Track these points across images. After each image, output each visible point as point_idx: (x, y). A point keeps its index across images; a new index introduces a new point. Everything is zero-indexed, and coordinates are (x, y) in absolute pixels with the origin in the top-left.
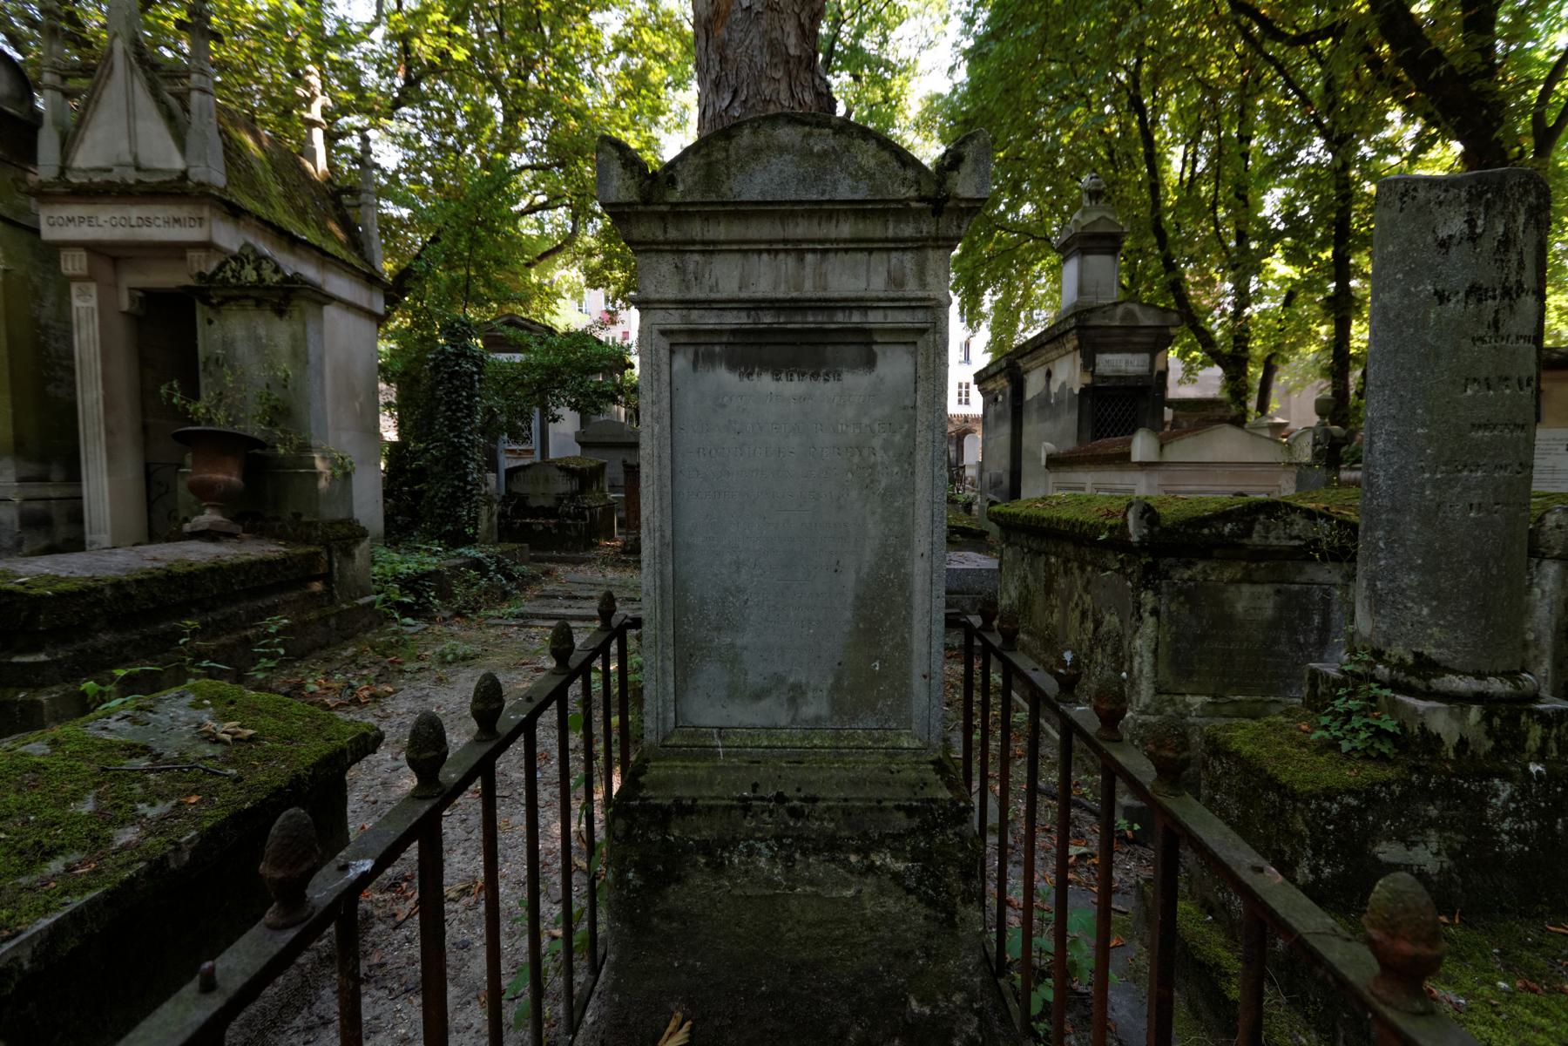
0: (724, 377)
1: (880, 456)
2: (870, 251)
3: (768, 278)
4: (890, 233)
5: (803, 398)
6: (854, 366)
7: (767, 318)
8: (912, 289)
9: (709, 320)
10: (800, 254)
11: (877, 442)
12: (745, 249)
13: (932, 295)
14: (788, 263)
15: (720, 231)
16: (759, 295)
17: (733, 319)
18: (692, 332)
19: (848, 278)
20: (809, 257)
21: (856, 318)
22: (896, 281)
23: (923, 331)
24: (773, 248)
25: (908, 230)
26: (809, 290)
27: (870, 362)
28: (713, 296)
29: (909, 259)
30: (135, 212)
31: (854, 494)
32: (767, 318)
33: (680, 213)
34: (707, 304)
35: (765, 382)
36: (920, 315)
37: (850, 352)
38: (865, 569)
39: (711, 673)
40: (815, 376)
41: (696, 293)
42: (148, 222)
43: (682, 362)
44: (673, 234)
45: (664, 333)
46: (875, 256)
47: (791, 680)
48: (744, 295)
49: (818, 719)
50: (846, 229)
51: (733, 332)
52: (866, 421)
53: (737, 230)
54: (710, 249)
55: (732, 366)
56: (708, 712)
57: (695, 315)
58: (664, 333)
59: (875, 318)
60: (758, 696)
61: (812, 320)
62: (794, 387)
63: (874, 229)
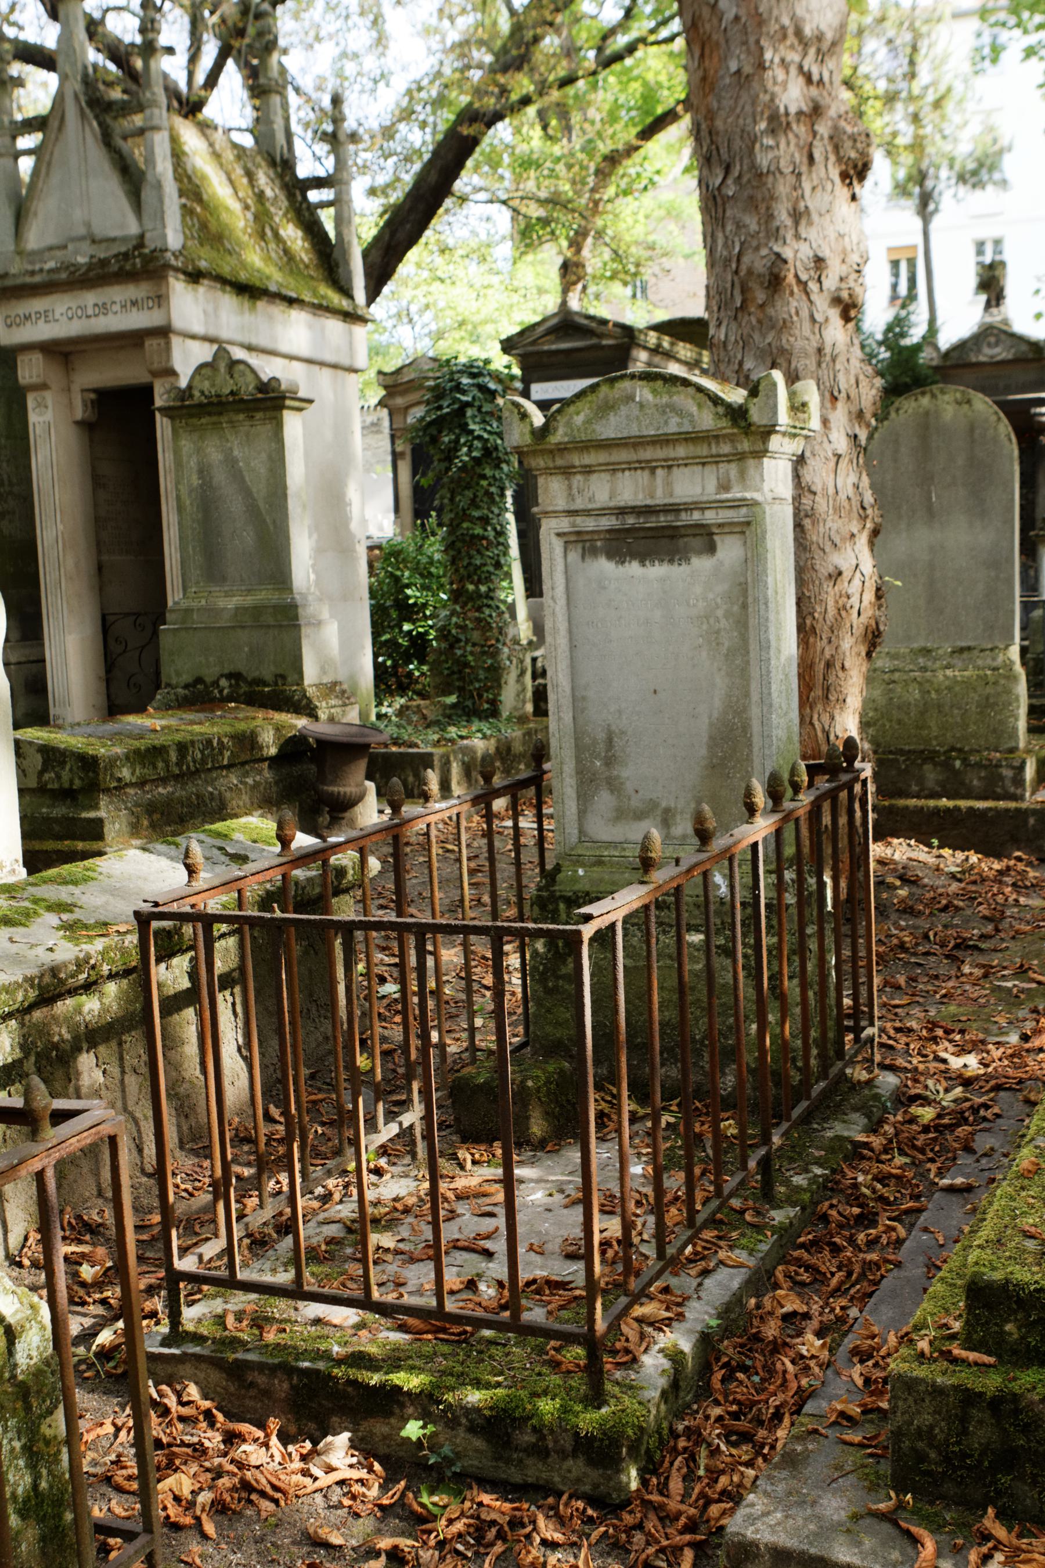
0: (604, 566)
1: (724, 623)
2: (704, 464)
3: (630, 489)
4: (714, 451)
5: (663, 580)
6: (699, 553)
7: (631, 520)
8: (736, 493)
9: (589, 524)
10: (653, 470)
11: (720, 613)
12: (613, 469)
13: (748, 495)
14: (643, 477)
15: (590, 458)
16: (622, 504)
17: (607, 522)
18: (578, 533)
19: (690, 485)
20: (660, 472)
21: (696, 515)
22: (724, 486)
23: (748, 523)
24: (633, 467)
25: (726, 448)
26: (660, 498)
27: (711, 549)
28: (590, 506)
29: (733, 469)
30: (90, 298)
31: (704, 654)
32: (631, 520)
33: (562, 449)
34: (587, 513)
35: (634, 568)
36: (744, 511)
37: (697, 542)
38: (715, 714)
39: (604, 800)
40: (671, 561)
41: (579, 504)
42: (103, 309)
43: (574, 556)
44: (559, 462)
45: (558, 535)
46: (708, 468)
47: (664, 804)
48: (612, 504)
49: (684, 837)
50: (681, 451)
51: (609, 531)
52: (711, 596)
53: (602, 457)
54: (588, 471)
55: (610, 556)
56: (602, 829)
57: (579, 520)
58: (558, 535)
59: (710, 517)
60: (639, 816)
61: (663, 520)
62: (657, 570)
63: (703, 450)
